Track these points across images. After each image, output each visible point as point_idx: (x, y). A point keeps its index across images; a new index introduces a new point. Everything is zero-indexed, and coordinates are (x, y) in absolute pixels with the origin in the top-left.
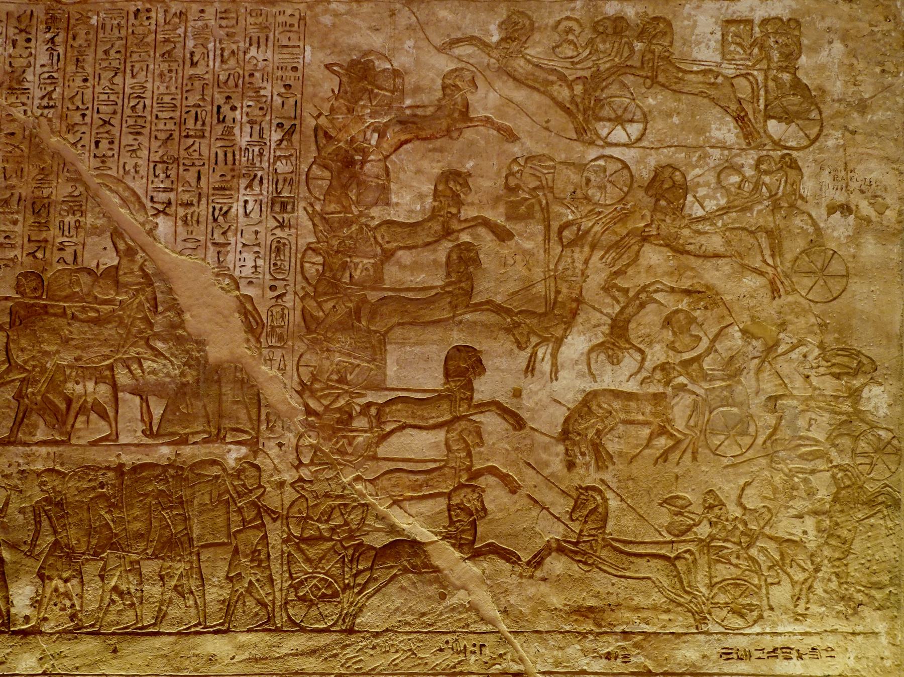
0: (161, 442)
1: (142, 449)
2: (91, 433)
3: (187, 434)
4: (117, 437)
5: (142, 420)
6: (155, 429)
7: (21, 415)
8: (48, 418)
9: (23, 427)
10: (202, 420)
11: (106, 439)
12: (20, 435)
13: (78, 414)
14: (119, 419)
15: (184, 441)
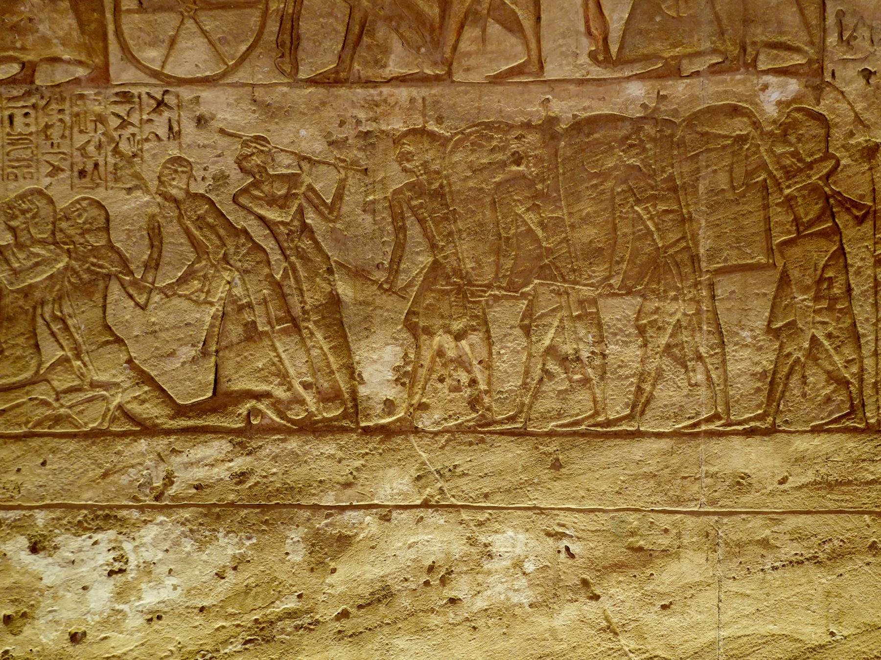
0: (627, 73)
1: (590, 88)
2: (491, 60)
3: (678, 58)
4: (542, 68)
5: (589, 33)
6: (614, 49)
7: (356, 29)
8: (408, 34)
9: (362, 51)
10: (707, 29)
11: (518, 71)
12: (356, 66)
13: (462, 27)
14: (544, 32)
15: (674, 72)
